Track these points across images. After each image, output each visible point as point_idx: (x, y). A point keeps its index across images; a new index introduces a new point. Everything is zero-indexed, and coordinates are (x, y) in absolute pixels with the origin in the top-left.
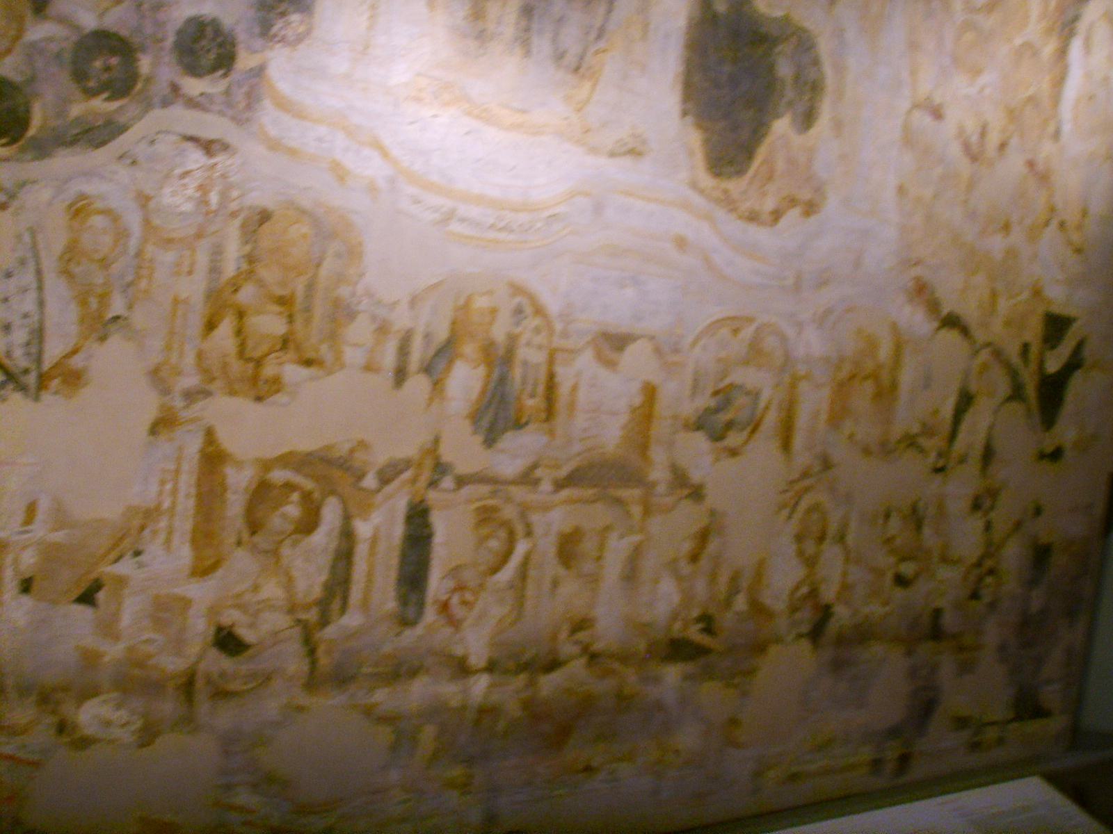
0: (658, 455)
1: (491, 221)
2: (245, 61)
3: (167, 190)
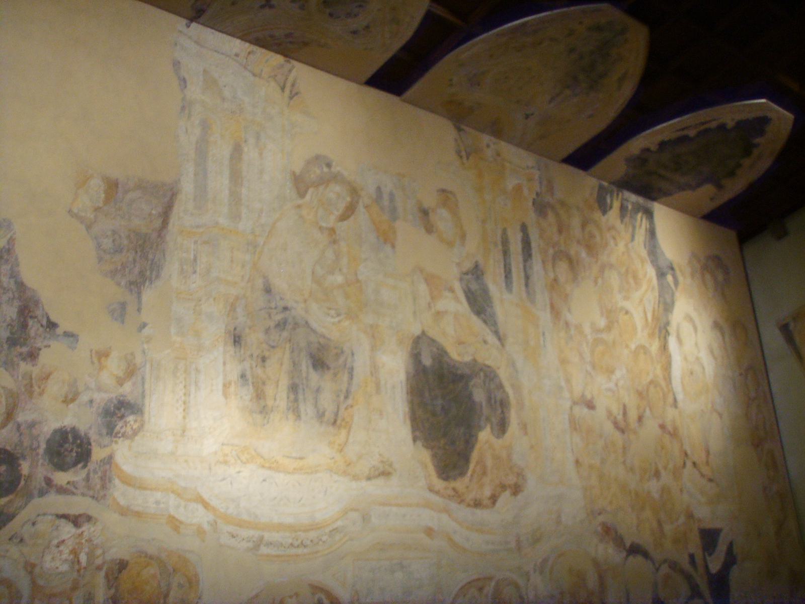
1: (290, 541)
2: (98, 454)
3: (48, 558)
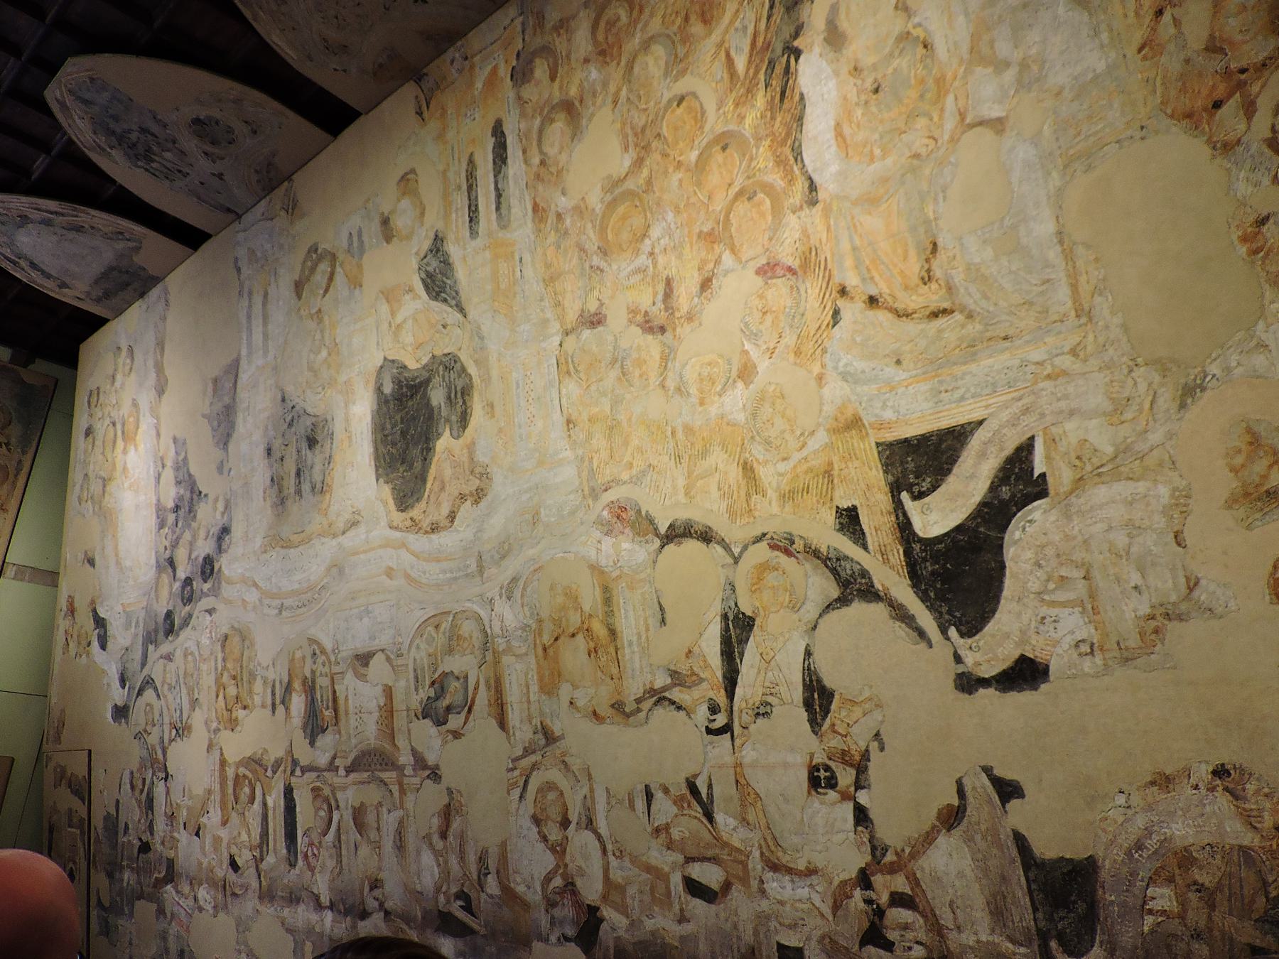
0: (401, 742)
